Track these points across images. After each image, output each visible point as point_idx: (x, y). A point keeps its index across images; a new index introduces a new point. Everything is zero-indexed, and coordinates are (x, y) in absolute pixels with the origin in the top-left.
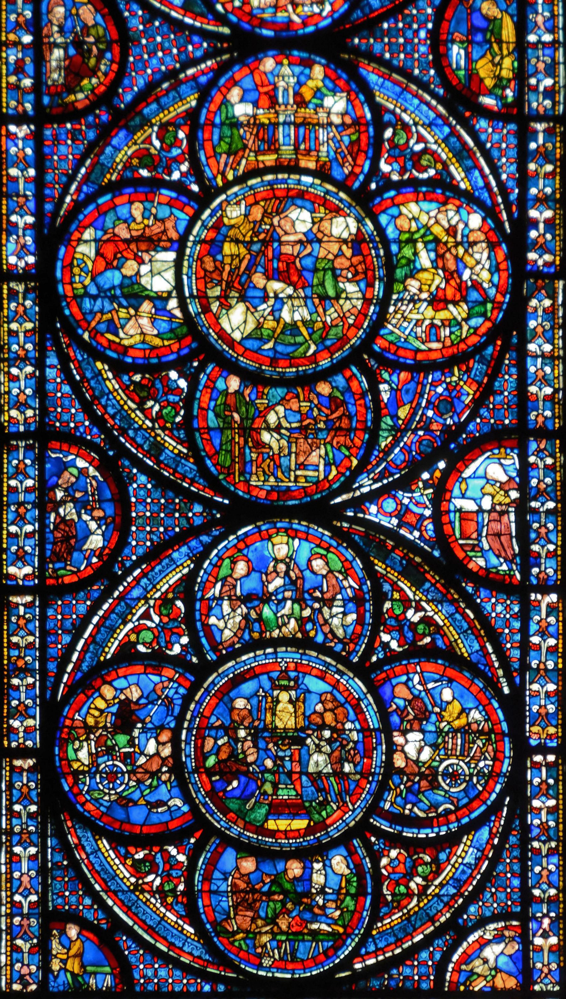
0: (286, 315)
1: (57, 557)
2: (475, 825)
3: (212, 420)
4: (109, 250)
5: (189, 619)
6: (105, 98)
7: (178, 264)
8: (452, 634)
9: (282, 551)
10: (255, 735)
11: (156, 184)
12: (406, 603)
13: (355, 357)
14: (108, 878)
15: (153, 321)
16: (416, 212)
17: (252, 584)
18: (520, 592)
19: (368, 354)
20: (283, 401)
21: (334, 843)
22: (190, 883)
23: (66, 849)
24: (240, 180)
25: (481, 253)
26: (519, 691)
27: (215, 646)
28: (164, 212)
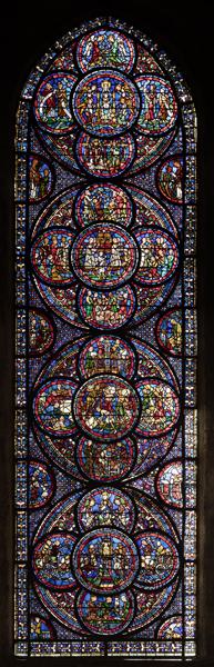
0: (107, 421)
1: (33, 499)
2: (167, 586)
3: (83, 455)
4: (50, 400)
5: (75, 519)
6: (50, 350)
7: (72, 404)
8: (160, 524)
9: (105, 498)
10: (97, 557)
11: (65, 378)
12: (145, 514)
13: (129, 435)
14: (49, 603)
15: (64, 422)
16: (149, 387)
17: (96, 508)
18: (183, 511)
19: (133, 434)
20: (106, 449)
21: (122, 592)
22: (75, 604)
23: (36, 594)
24: (92, 377)
25: (171, 400)
26: (182, 542)
27: (84, 528)
28: (68, 387)
